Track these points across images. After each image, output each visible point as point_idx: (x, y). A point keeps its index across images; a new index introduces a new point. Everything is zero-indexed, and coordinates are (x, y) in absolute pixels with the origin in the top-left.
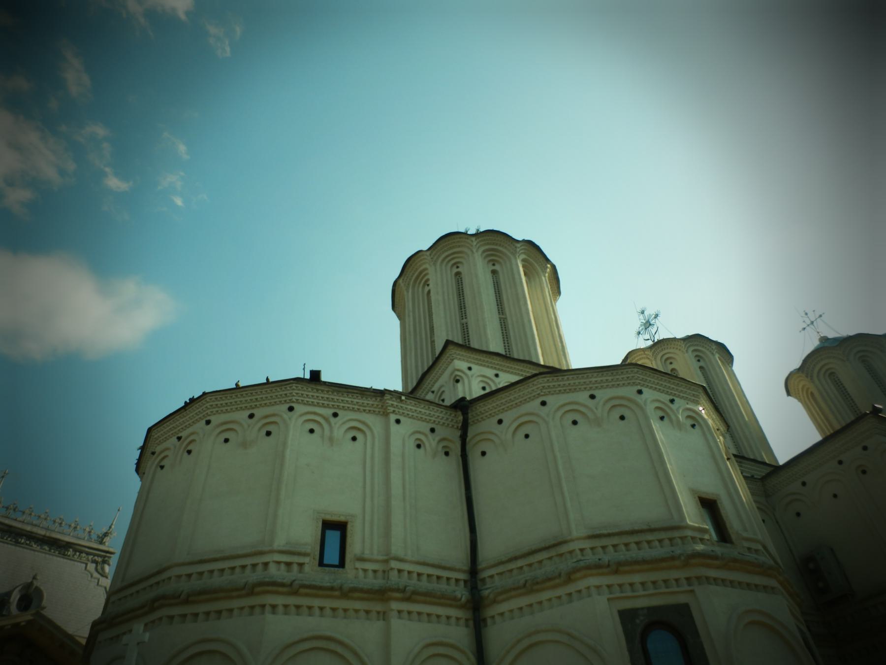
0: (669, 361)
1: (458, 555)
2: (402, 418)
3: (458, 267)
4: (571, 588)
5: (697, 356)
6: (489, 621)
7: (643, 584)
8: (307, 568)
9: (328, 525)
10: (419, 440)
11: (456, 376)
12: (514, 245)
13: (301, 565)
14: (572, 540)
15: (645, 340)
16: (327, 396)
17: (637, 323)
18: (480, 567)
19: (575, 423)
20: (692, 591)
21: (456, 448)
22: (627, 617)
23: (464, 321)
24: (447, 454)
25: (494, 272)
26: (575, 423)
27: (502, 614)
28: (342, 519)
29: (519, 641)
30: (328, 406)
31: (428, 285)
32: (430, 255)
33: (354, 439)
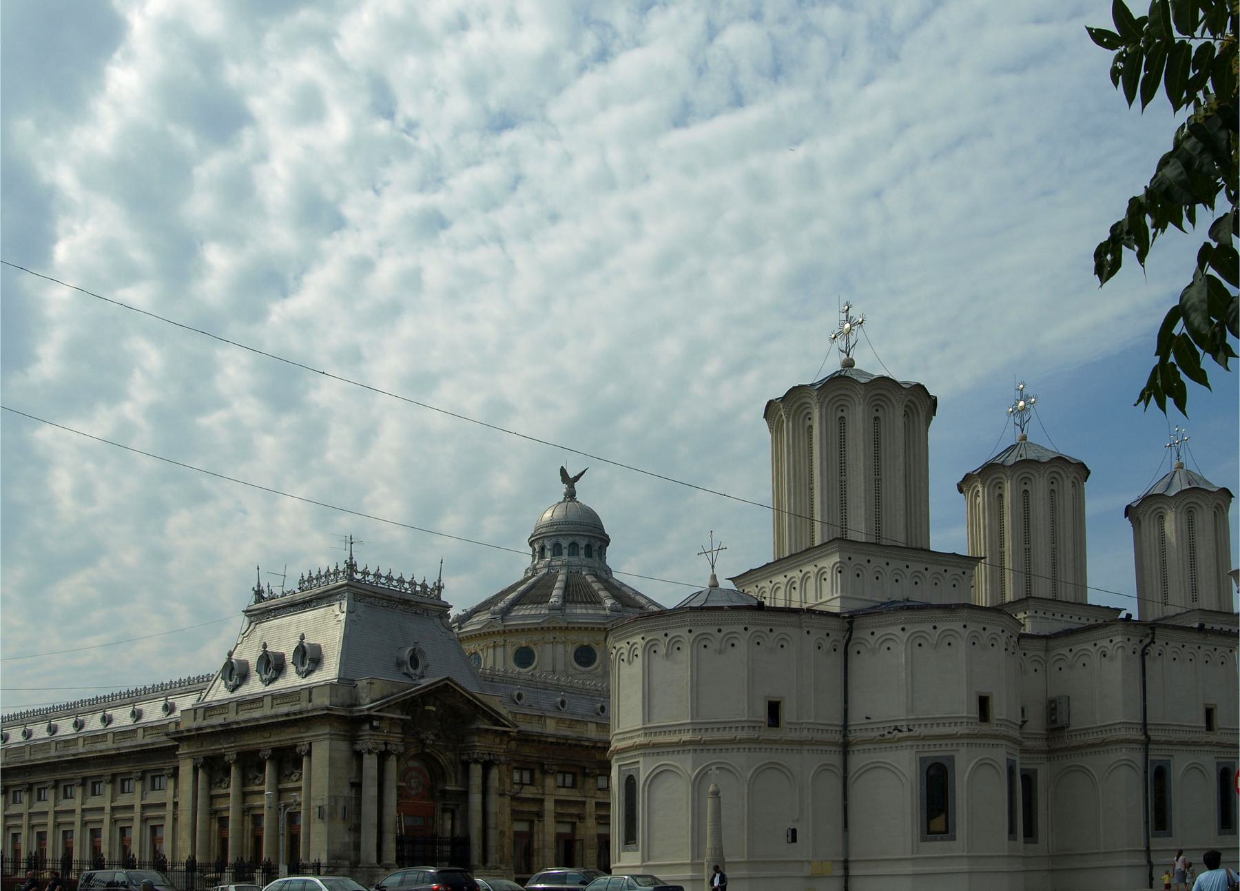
2: (810, 630)
10: (820, 643)
18: (849, 723)
24: (835, 650)
28: (777, 700)
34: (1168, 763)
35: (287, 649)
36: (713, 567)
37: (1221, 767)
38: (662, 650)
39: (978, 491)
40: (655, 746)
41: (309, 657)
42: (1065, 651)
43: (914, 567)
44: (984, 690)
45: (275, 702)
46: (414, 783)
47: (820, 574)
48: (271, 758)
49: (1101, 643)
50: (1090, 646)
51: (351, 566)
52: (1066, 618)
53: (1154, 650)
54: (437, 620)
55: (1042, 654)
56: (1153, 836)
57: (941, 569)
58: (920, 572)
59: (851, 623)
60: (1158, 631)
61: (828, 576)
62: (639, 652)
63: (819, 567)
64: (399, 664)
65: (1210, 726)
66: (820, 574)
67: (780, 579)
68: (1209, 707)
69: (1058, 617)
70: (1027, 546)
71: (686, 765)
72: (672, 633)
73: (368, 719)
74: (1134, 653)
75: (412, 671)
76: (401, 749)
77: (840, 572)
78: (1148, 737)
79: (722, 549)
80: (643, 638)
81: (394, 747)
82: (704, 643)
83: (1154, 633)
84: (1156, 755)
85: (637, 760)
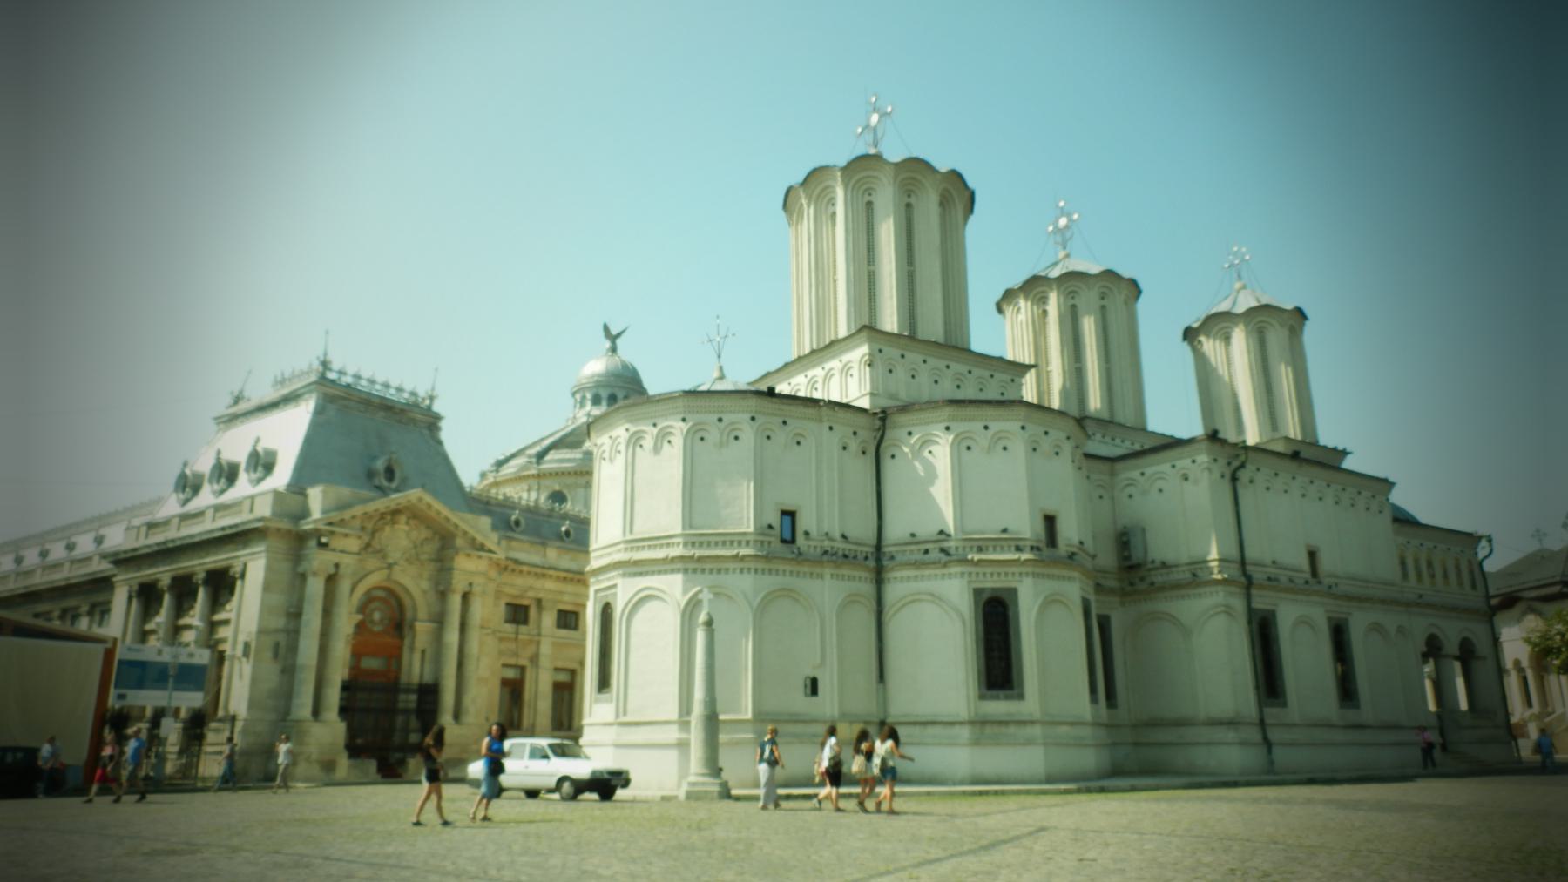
4: (946, 571)
5: (1103, 293)
6: (886, 581)
8: (772, 545)
9: (784, 513)
13: (770, 543)
22: (977, 592)
24: (864, 453)
25: (908, 205)
29: (905, 597)
35: (240, 456)
36: (719, 357)
38: (648, 442)
40: (637, 563)
41: (263, 463)
42: (1135, 474)
43: (955, 367)
44: (1051, 508)
45: (218, 515)
46: (377, 616)
47: (846, 370)
48: (207, 582)
49: (1179, 464)
50: (1166, 467)
51: (325, 364)
53: (1244, 475)
54: (426, 432)
58: (961, 374)
59: (883, 420)
61: (855, 372)
62: (622, 447)
63: (844, 362)
64: (371, 474)
65: (1314, 572)
66: (846, 370)
69: (1118, 441)
70: (1078, 365)
71: (673, 586)
72: (662, 424)
73: (317, 534)
75: (385, 483)
77: (870, 365)
78: (1248, 577)
80: (627, 430)
82: (700, 434)
84: (1261, 602)
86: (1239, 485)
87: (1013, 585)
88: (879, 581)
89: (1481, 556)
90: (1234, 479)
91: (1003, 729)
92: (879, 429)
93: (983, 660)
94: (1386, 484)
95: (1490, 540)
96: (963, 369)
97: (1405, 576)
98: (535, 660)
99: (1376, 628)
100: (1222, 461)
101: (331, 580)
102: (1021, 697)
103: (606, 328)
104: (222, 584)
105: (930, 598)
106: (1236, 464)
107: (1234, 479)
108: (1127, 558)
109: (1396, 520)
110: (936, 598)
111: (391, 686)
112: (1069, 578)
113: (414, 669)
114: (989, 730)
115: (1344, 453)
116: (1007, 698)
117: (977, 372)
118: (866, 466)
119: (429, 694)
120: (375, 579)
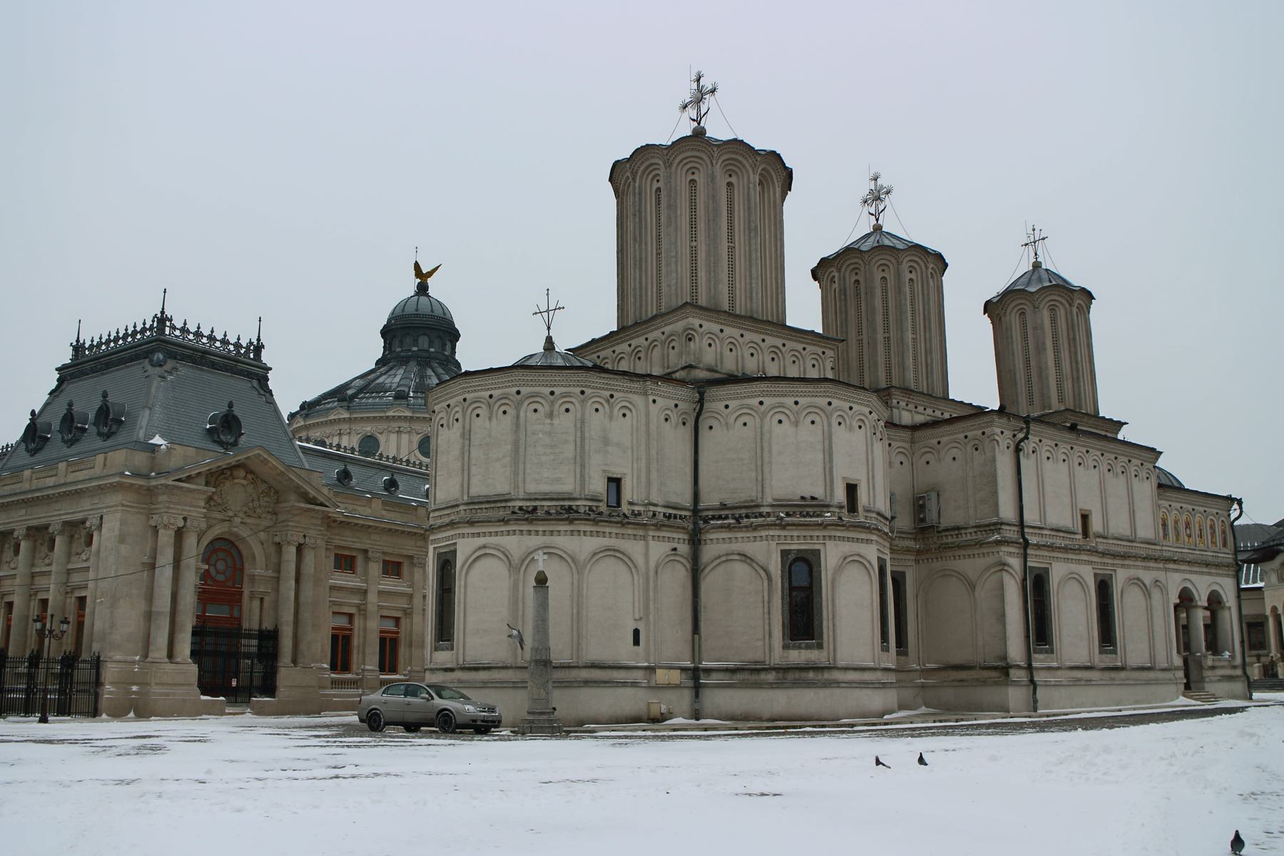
0: (884, 267)
1: (686, 501)
3: (693, 173)
6: (703, 542)
7: (798, 536)
9: (610, 480)
11: (689, 334)
12: (755, 157)
14: (762, 506)
15: (870, 213)
16: (606, 382)
17: (866, 187)
19: (780, 422)
20: (825, 543)
21: (691, 422)
22: (784, 553)
23: (694, 244)
24: (684, 424)
25: (729, 184)
26: (780, 422)
27: (711, 540)
28: (619, 476)
29: (719, 557)
30: (607, 389)
31: (658, 181)
32: (667, 155)
33: (624, 415)
34: (1046, 570)
36: (549, 328)
37: (1099, 579)
39: (834, 277)
43: (771, 341)
45: (70, 469)
52: (929, 411)
53: (1028, 446)
55: (907, 445)
56: (1035, 652)
57: (800, 347)
60: (1033, 427)
67: (624, 347)
68: (1084, 513)
69: (920, 409)
70: (886, 335)
74: (1008, 448)
76: (204, 526)
78: (1026, 541)
79: (559, 308)
81: (195, 524)
83: (1028, 428)
85: (454, 541)
86: (1021, 453)
87: (817, 547)
88: (695, 541)
89: (1232, 518)
90: (1018, 450)
91: (804, 675)
92: (698, 402)
93: (787, 614)
94: (1155, 454)
95: (1240, 502)
96: (779, 342)
97: (1165, 535)
98: (362, 609)
99: (1138, 582)
100: (1008, 433)
101: (179, 534)
102: (820, 646)
103: (417, 266)
104: (80, 533)
105: (743, 558)
106: (1021, 436)
107: (1018, 450)
108: (923, 520)
109: (1160, 486)
110: (745, 558)
111: (234, 631)
112: (868, 541)
113: (252, 618)
114: (790, 676)
115: (1120, 424)
116: (808, 647)
117: (790, 344)
118: (686, 433)
119: (269, 638)
120: (216, 531)
